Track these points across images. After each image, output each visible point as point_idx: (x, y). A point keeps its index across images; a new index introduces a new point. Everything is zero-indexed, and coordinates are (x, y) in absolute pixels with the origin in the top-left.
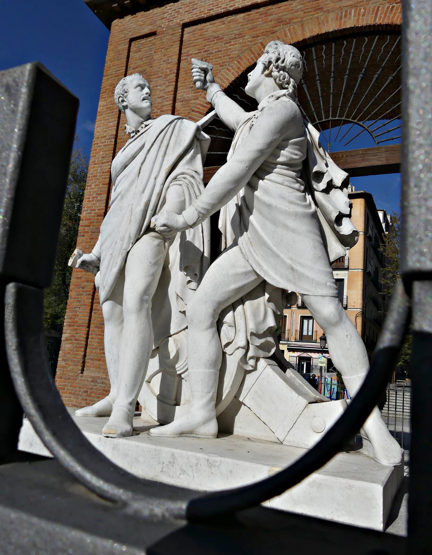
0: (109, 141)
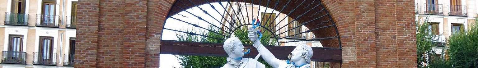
0: (94, 8)
